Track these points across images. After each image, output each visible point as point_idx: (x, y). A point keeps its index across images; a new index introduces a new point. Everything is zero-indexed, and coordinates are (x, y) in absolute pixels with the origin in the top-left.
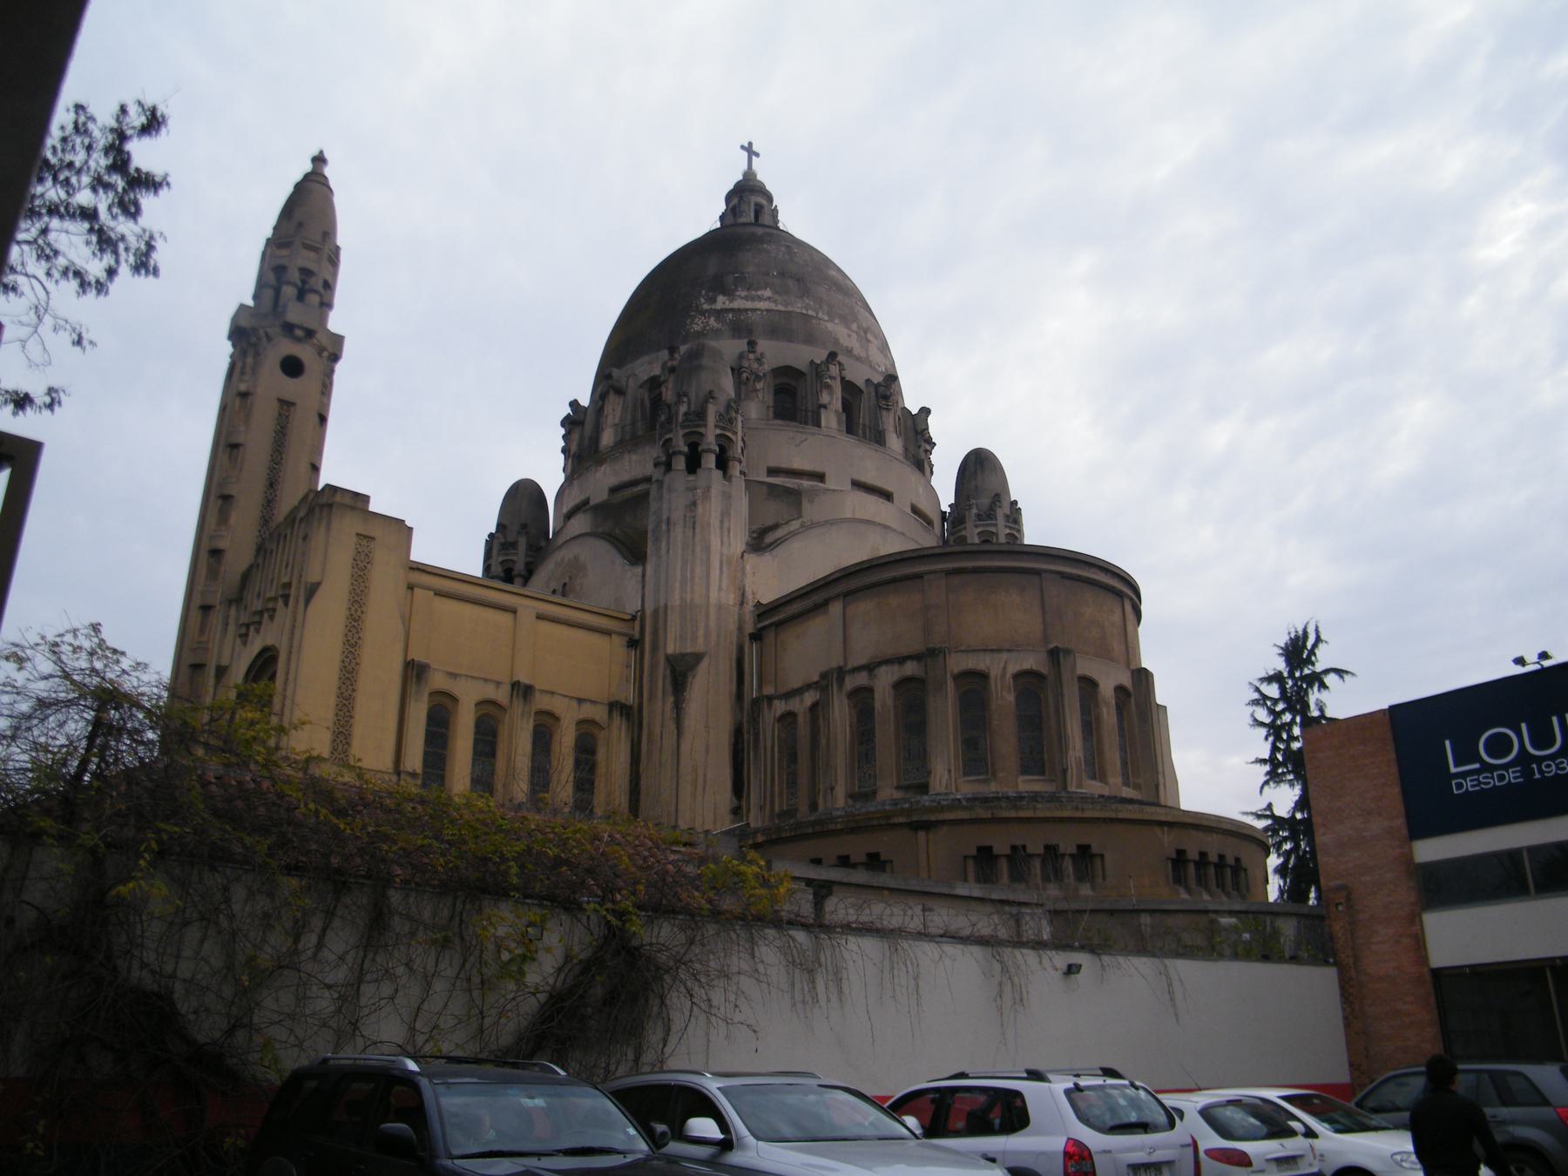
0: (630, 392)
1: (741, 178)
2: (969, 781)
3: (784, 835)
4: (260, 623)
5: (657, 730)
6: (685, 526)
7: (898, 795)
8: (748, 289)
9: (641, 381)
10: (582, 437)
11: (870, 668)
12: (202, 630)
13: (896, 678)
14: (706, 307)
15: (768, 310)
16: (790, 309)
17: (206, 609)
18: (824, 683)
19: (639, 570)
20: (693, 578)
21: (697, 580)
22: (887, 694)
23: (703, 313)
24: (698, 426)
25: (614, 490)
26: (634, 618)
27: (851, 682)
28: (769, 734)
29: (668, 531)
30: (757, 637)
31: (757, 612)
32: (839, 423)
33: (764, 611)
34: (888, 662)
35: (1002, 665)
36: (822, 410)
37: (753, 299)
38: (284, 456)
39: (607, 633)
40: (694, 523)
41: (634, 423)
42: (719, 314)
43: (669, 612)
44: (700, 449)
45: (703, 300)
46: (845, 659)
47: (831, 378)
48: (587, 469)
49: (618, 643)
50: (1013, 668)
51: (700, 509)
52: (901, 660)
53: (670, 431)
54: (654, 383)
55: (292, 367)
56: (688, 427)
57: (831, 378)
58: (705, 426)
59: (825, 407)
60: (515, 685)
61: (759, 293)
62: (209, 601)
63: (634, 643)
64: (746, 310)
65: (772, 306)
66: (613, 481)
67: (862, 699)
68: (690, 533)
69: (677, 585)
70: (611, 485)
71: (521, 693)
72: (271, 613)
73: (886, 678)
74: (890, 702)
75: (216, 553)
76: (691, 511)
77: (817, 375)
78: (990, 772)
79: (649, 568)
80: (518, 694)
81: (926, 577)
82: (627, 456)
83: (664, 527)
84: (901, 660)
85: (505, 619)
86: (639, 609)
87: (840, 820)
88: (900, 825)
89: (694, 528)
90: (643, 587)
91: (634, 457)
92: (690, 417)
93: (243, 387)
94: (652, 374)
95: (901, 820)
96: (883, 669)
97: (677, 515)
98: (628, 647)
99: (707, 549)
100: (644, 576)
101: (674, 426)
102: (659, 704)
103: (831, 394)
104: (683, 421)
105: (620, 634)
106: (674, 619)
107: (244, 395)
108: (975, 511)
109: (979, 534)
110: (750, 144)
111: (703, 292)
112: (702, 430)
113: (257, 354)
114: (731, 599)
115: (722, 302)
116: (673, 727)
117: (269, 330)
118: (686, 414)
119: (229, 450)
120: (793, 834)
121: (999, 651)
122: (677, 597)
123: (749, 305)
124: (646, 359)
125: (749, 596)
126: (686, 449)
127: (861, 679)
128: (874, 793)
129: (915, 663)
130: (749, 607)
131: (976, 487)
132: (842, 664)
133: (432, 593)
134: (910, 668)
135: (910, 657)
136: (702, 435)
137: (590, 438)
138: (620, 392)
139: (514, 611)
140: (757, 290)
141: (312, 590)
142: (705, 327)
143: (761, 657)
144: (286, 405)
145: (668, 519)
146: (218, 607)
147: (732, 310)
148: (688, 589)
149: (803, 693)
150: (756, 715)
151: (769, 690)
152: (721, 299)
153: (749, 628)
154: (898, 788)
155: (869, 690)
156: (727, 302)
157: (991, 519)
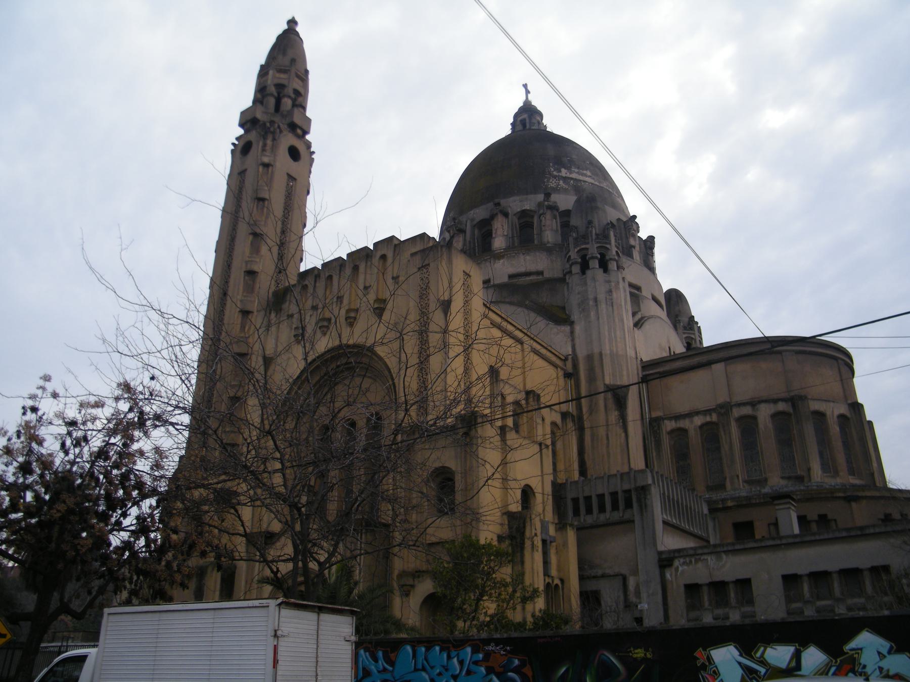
0: (510, 216)
1: (522, 105)
2: (826, 476)
3: (754, 501)
4: (328, 327)
5: (602, 432)
6: (607, 304)
7: (783, 482)
8: (578, 168)
9: (515, 212)
10: (465, 240)
11: (753, 403)
12: (243, 327)
13: (773, 411)
14: (555, 173)
15: (592, 184)
16: (602, 185)
17: (245, 313)
18: (723, 411)
19: (567, 329)
20: (616, 337)
21: (619, 339)
22: (767, 421)
23: (555, 177)
24: (606, 243)
25: (511, 277)
26: (566, 359)
27: (737, 412)
28: (734, 437)
29: (597, 305)
30: (645, 380)
31: (643, 365)
32: (640, 259)
33: (646, 366)
34: (766, 401)
35: (831, 409)
36: (633, 249)
37: (583, 175)
38: (290, 214)
39: (555, 366)
40: (612, 303)
41: (513, 237)
42: (565, 179)
43: (604, 358)
44: (607, 258)
45: (552, 170)
46: (730, 398)
47: (634, 230)
48: (486, 260)
49: (561, 373)
50: (836, 413)
51: (615, 295)
52: (775, 401)
53: (588, 243)
54: (524, 214)
55: (294, 154)
56: (600, 243)
57: (635, 231)
58: (610, 244)
59: (634, 247)
60: (528, 393)
61: (585, 172)
62: (248, 308)
63: (567, 375)
64: (581, 181)
65: (592, 181)
66: (512, 270)
67: (748, 425)
68: (610, 308)
69: (607, 340)
70: (511, 273)
71: (536, 398)
72: (352, 320)
73: (764, 413)
74: (770, 425)
75: (251, 273)
76: (610, 295)
77: (625, 228)
78: (832, 470)
79: (578, 328)
80: (534, 399)
81: (784, 354)
82: (522, 257)
83: (591, 303)
84: (775, 401)
85: (519, 346)
86: (570, 353)
87: (798, 493)
88: (839, 497)
89: (612, 306)
90: (573, 340)
91: (528, 257)
92: (600, 237)
93: (266, 160)
94: (524, 208)
95: (841, 495)
96: (763, 407)
97: (601, 296)
98: (565, 377)
99: (622, 320)
100: (572, 332)
101: (590, 240)
102: (601, 417)
103: (635, 240)
104: (596, 239)
105: (562, 369)
106: (607, 361)
107: (266, 166)
108: (682, 324)
109: (686, 338)
110: (526, 84)
111: (551, 164)
112: (608, 246)
113: (274, 139)
114: (634, 356)
115: (564, 173)
116: (620, 431)
117: (281, 125)
118: (596, 234)
119: (256, 201)
120: (762, 501)
121: (829, 401)
122: (607, 347)
123: (581, 178)
124: (517, 198)
125: (638, 355)
126: (599, 256)
127: (747, 410)
128: (766, 480)
129: (784, 403)
130: (639, 362)
131: (680, 311)
132: (728, 400)
133: (489, 322)
134: (781, 406)
135: (783, 400)
136: (608, 249)
137: (470, 242)
138: (506, 215)
139: (522, 343)
140: (583, 169)
141: (446, 306)
142: (557, 187)
143: (648, 392)
144: (291, 178)
145: (596, 300)
146: (255, 313)
147: (572, 179)
148: (614, 345)
149: (693, 416)
150: (656, 428)
151: (659, 414)
152: (563, 170)
153: (641, 376)
154: (782, 478)
155: (754, 418)
156: (568, 174)
157: (692, 330)
